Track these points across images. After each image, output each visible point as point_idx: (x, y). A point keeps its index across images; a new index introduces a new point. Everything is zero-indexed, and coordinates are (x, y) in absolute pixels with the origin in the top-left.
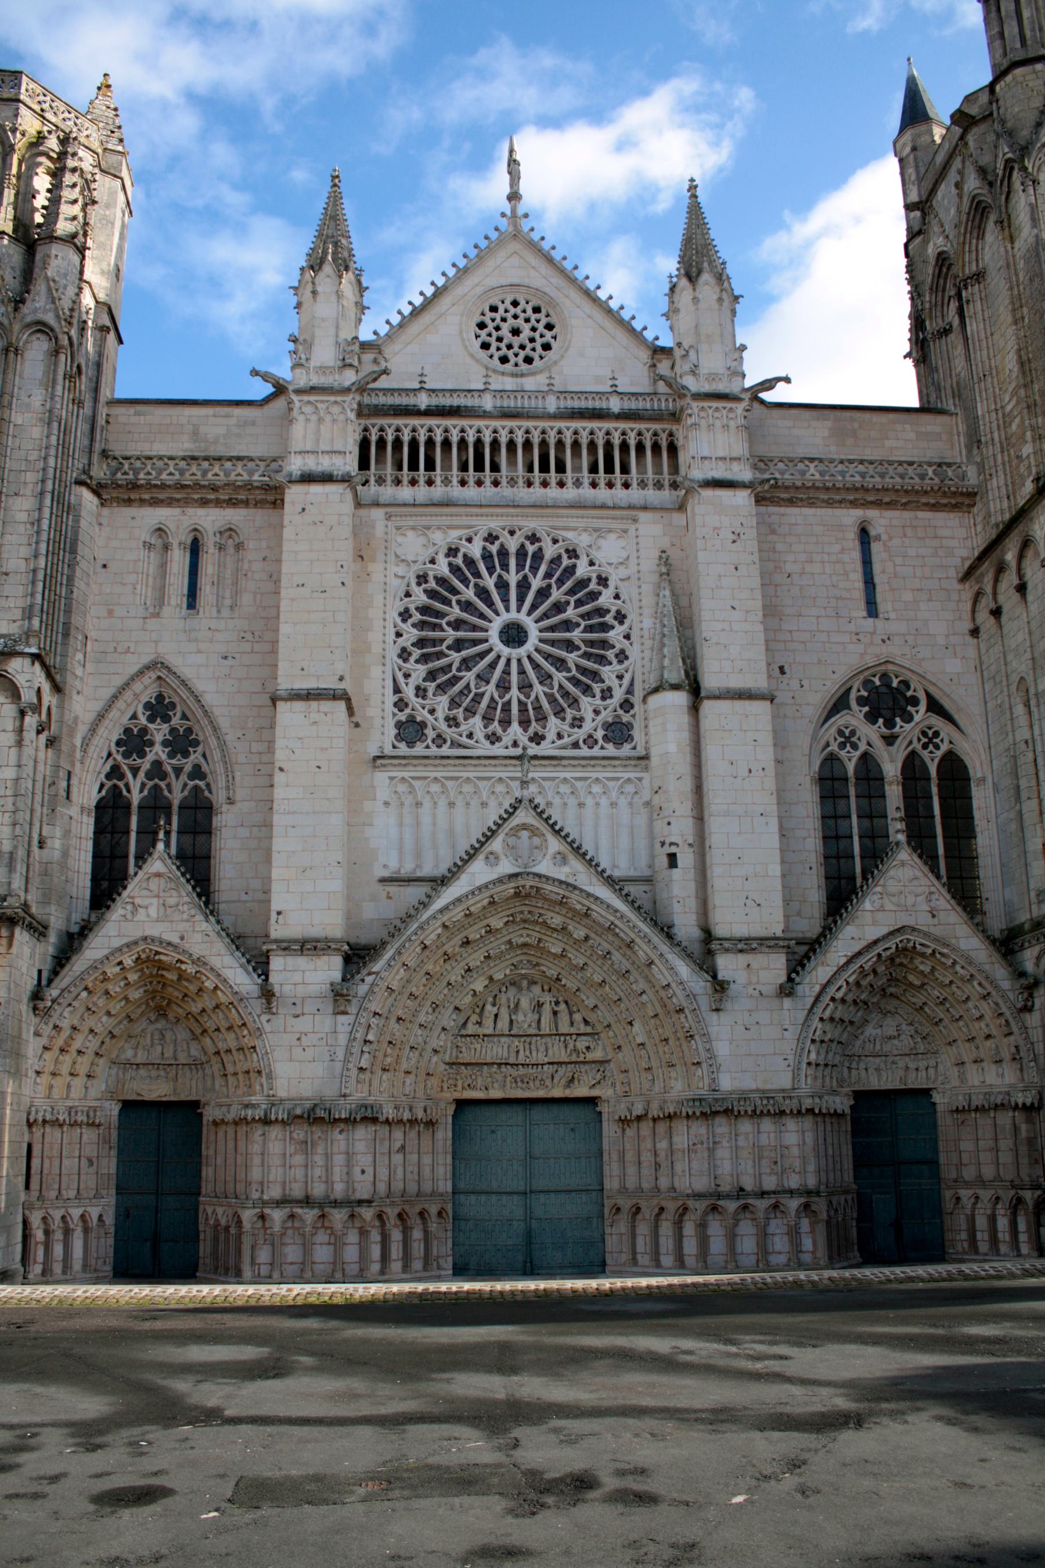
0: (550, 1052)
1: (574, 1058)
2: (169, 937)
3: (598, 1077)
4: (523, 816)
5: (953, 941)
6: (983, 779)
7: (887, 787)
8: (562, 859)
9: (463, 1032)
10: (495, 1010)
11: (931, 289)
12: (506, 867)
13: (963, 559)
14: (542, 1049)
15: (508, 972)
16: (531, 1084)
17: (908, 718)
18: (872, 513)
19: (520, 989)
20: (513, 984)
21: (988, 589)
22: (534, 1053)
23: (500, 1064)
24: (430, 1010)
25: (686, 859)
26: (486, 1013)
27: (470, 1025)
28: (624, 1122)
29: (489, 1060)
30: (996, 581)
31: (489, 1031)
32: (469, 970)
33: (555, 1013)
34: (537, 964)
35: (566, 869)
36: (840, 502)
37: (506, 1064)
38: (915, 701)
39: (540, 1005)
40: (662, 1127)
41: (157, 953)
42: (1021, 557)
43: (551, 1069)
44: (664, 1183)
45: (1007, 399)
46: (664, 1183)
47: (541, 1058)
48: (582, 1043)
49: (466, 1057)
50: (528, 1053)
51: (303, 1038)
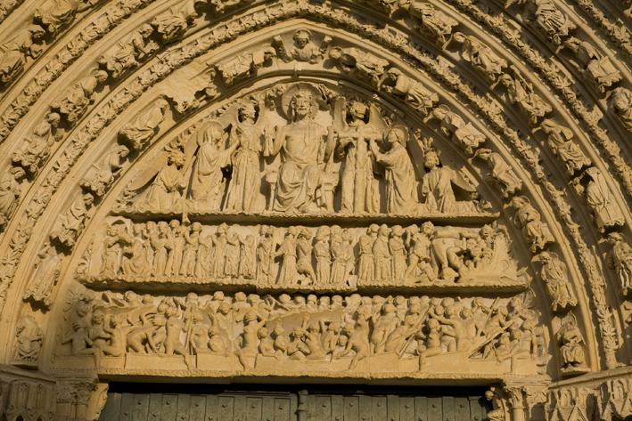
0: (366, 260)
1: (430, 278)
3: (495, 329)
9: (140, 206)
10: (224, 158)
14: (345, 253)
15: (259, 59)
16: (314, 339)
19: (293, 117)
20: (274, 102)
22: (324, 264)
23: (230, 291)
24: (44, 127)
26: (203, 166)
27: (158, 190)
29: (202, 278)
31: (212, 207)
32: (156, 36)
33: (380, 170)
34: (336, 42)
37: (249, 290)
39: (341, 153)
43: (370, 306)
47: (343, 277)
48: (449, 243)
49: (147, 267)
50: (306, 261)
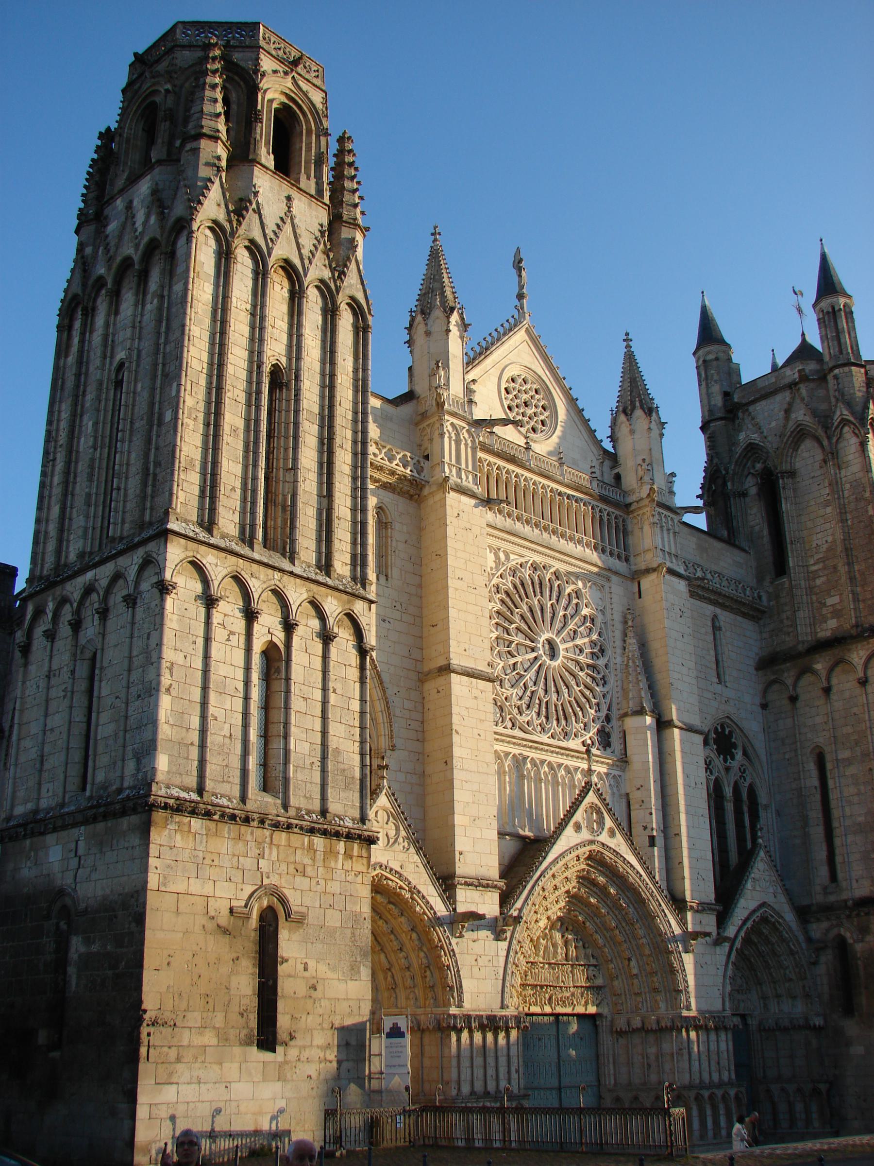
2: (396, 866)
4: (591, 797)
5: (783, 914)
6: (766, 807)
7: (726, 804)
8: (612, 834)
11: (736, 462)
12: (585, 835)
13: (757, 654)
17: (733, 758)
18: (718, 611)
21: (789, 681)
25: (659, 841)
28: (621, 1033)
30: (798, 678)
35: (614, 841)
36: (705, 598)
38: (734, 746)
40: (651, 1038)
41: (387, 878)
42: (831, 670)
44: (654, 1078)
45: (812, 562)
46: (654, 1078)
51: (479, 958)
